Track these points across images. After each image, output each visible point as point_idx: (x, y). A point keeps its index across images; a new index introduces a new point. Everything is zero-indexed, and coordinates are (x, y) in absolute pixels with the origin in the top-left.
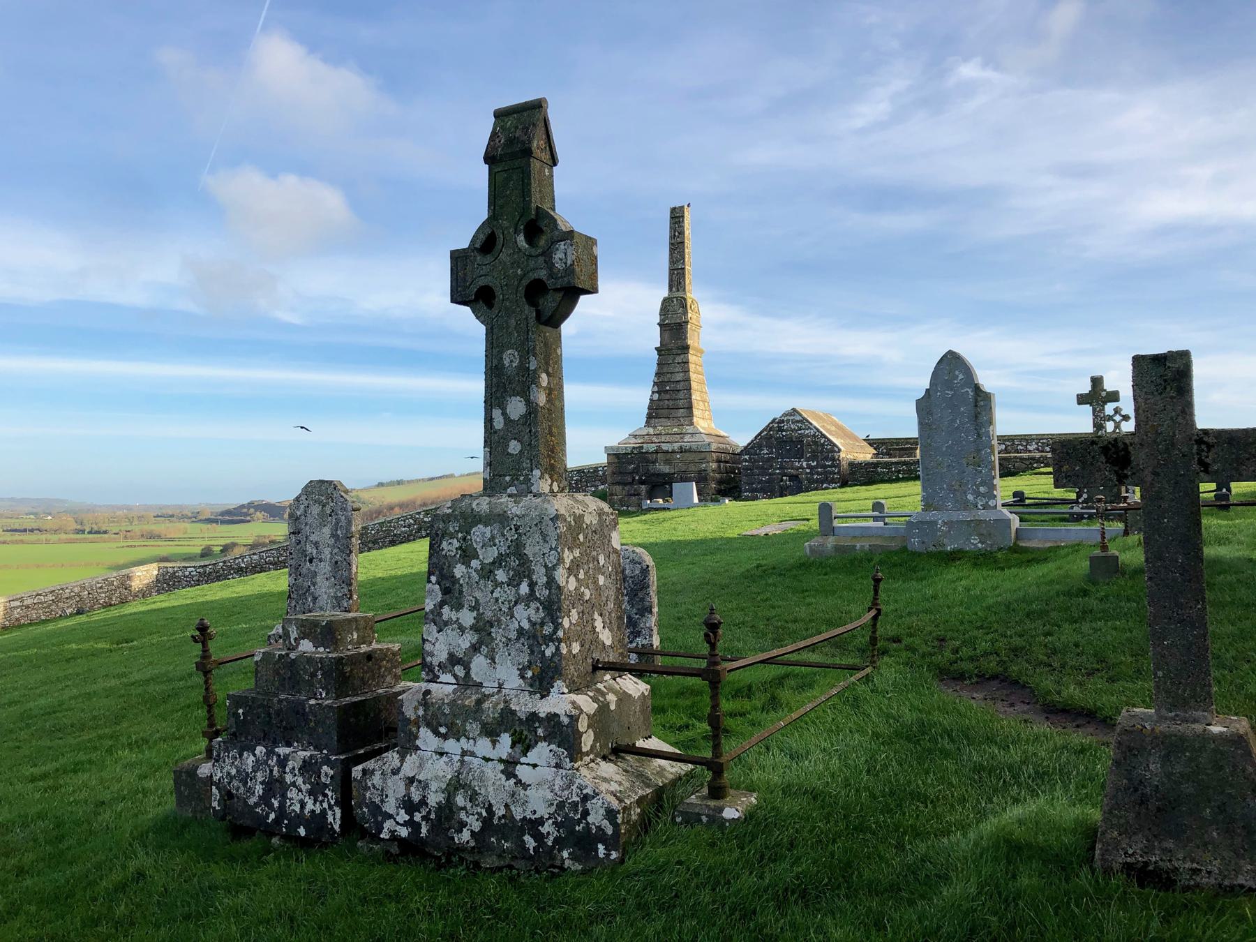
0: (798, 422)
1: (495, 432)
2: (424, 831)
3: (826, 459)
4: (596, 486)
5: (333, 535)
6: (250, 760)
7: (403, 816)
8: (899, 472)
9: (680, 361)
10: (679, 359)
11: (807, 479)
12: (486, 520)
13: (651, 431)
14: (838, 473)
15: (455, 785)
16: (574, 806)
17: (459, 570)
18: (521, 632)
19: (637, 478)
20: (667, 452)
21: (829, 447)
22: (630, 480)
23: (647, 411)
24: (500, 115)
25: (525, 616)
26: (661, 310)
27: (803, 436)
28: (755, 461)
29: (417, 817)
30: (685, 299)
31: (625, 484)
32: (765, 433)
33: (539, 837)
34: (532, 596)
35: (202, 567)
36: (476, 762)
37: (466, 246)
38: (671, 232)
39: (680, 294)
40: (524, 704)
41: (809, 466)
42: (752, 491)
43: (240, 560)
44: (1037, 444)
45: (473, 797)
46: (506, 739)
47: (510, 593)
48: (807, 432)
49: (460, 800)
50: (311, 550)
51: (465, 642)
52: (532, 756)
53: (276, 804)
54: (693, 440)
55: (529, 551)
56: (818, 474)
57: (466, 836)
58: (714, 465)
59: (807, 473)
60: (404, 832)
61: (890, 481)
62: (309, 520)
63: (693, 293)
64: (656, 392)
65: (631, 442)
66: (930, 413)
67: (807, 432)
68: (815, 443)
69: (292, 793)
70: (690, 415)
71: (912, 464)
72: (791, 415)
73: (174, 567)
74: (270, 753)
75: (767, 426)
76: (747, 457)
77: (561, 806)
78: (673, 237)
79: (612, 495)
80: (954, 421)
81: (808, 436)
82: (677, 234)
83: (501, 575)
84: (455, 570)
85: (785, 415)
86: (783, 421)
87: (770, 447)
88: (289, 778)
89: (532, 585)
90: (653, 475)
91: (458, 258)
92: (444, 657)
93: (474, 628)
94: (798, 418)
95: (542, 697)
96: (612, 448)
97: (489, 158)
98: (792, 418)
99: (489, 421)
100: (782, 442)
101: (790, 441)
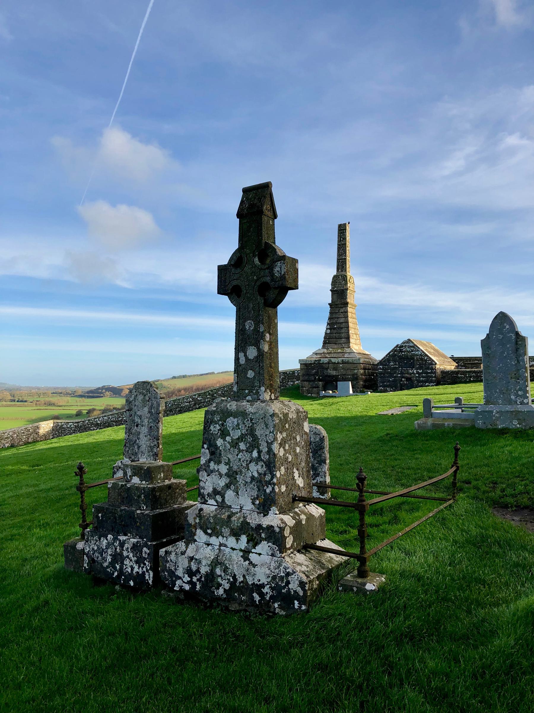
0: (411, 347)
1: (240, 365)
2: (198, 587)
3: (428, 368)
4: (294, 382)
5: (149, 412)
6: (104, 542)
7: (187, 578)
8: (471, 377)
9: (343, 311)
10: (342, 310)
11: (416, 380)
12: (235, 414)
13: (325, 351)
14: (435, 377)
15: (216, 563)
16: (282, 578)
17: (219, 442)
18: (253, 478)
19: (317, 378)
20: (335, 363)
21: (430, 362)
22: (313, 379)
23: (323, 339)
24: (246, 191)
25: (255, 469)
26: (332, 282)
27: (414, 355)
29: (195, 579)
30: (346, 276)
31: (309, 381)
32: (392, 353)
33: (261, 595)
34: (259, 459)
35: (77, 423)
36: (228, 550)
37: (226, 263)
38: (338, 238)
39: (343, 273)
40: (254, 519)
41: (418, 373)
42: (384, 386)
43: (97, 419)
45: (225, 570)
46: (244, 538)
47: (247, 456)
48: (417, 353)
49: (218, 571)
50: (137, 419)
51: (222, 482)
52: (258, 549)
53: (118, 567)
54: (350, 356)
55: (258, 433)
56: (423, 377)
57: (221, 591)
58: (362, 371)
59: (417, 377)
60: (187, 587)
61: (466, 382)
62: (137, 403)
63: (351, 272)
64: (329, 329)
65: (314, 357)
66: (489, 348)
67: (417, 353)
68: (422, 359)
69: (127, 562)
70: (348, 342)
71: (478, 372)
73: (62, 423)
74: (115, 539)
75: (393, 349)
76: (381, 367)
77: (274, 578)
78: (339, 241)
79: (302, 387)
80: (503, 352)
82: (342, 239)
83: (242, 446)
84: (217, 442)
85: (404, 343)
86: (402, 346)
87: (395, 361)
88: (125, 553)
89: (259, 452)
90: (327, 376)
91: (221, 269)
92: (210, 490)
93: (228, 475)
94: (411, 345)
95: (265, 516)
96: (303, 360)
97: (239, 215)
98: (408, 344)
99: (237, 359)
100: (401, 358)
101: (406, 358)
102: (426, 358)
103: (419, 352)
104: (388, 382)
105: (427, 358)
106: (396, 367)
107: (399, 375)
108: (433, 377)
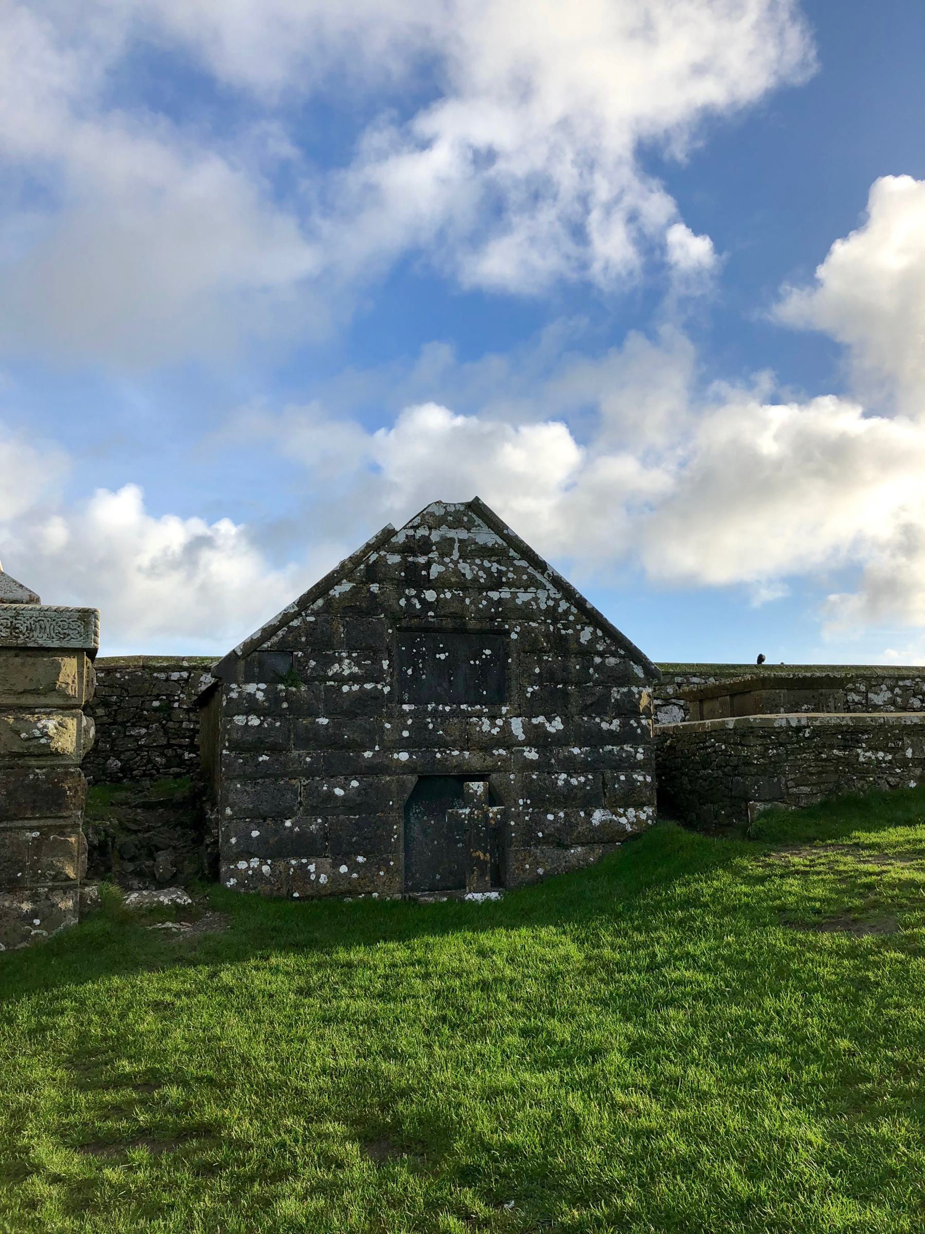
0: (486, 552)
3: (601, 707)
11: (528, 790)
21: (612, 661)
27: (507, 610)
28: (299, 709)
32: (346, 586)
41: (537, 738)
44: (891, 689)
48: (523, 597)
59: (531, 765)
67: (523, 597)
68: (560, 644)
72: (456, 524)
75: (356, 560)
81: (526, 613)
85: (428, 519)
86: (424, 546)
94: (486, 537)
98: (463, 534)
102: (586, 635)
103: (542, 595)
104: (313, 811)
105: (594, 640)
106: (376, 696)
107: (404, 756)
108: (636, 766)
